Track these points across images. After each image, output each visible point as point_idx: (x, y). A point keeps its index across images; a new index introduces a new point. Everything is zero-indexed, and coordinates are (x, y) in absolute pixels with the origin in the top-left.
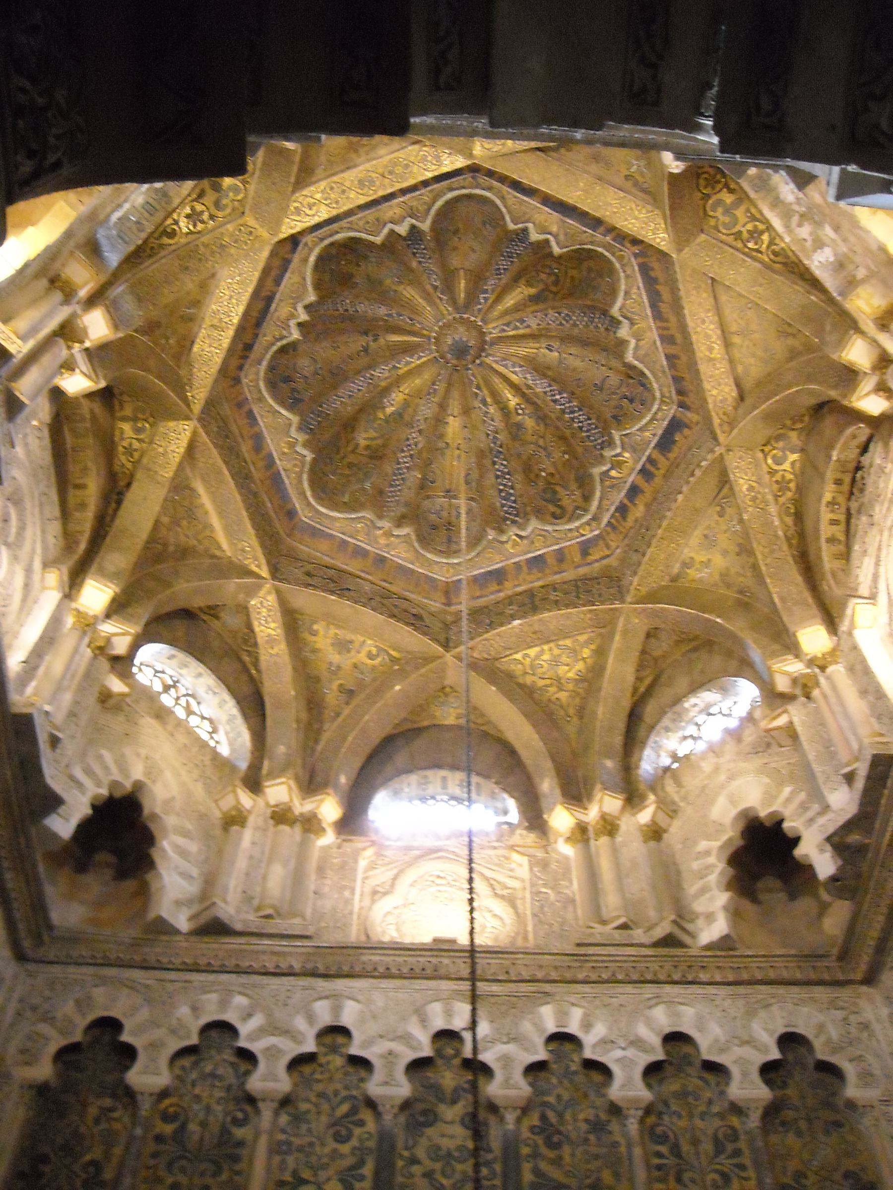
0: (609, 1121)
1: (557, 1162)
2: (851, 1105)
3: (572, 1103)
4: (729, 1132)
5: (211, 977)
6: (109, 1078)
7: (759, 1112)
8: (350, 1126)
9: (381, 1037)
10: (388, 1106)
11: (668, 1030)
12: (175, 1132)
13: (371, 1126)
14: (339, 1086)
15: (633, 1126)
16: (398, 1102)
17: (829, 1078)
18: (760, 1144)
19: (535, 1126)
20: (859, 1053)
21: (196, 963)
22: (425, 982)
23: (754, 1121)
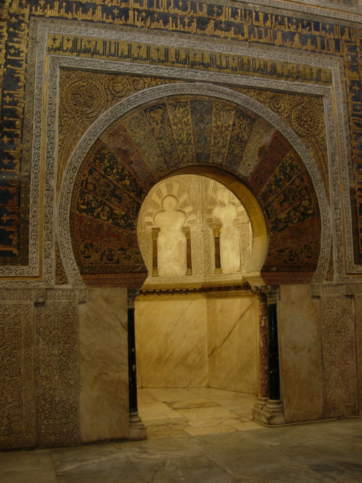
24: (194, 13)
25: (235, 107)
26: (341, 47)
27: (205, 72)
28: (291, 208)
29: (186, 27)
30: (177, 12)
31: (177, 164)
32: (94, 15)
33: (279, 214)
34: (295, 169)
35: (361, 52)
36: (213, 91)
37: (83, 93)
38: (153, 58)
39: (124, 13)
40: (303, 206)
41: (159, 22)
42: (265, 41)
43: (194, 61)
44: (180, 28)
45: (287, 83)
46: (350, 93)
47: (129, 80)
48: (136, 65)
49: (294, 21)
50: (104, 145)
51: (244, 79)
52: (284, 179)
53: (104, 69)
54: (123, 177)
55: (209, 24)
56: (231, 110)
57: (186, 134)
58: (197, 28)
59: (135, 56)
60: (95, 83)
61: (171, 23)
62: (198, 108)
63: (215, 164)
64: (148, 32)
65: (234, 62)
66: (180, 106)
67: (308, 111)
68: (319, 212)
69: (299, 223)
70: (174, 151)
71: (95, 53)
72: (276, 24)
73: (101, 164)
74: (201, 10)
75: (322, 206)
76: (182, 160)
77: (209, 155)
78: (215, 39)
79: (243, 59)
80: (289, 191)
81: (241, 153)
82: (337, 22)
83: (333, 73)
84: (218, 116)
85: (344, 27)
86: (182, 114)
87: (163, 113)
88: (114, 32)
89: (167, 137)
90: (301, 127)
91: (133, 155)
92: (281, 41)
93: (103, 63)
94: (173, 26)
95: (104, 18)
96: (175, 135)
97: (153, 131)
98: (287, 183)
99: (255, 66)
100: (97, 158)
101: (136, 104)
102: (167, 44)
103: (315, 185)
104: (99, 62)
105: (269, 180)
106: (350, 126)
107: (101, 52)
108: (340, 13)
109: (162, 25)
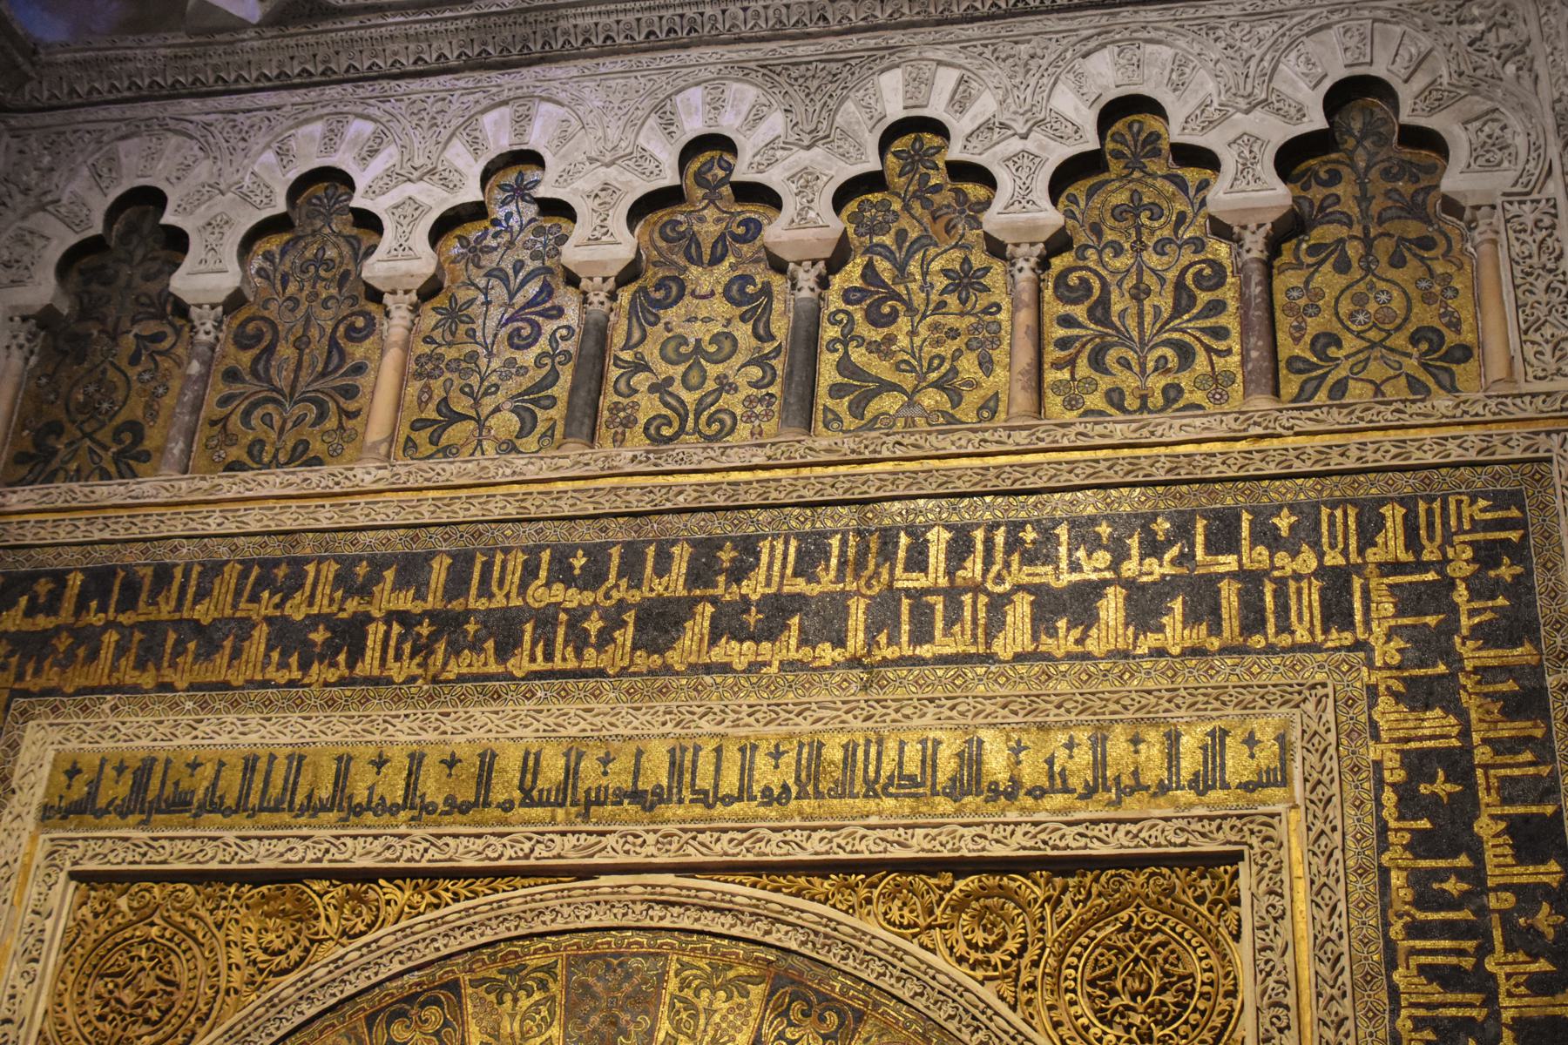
0: (987, 270)
1: (882, 349)
2: (1452, 206)
3: (924, 242)
4: (1207, 271)
5: (313, 94)
6: (153, 287)
7: (1262, 232)
8: (540, 320)
9: (592, 160)
10: (598, 280)
11: (1114, 94)
12: (256, 360)
13: (572, 316)
14: (525, 255)
15: (1025, 277)
16: (614, 270)
17: (1425, 155)
18: (1256, 290)
19: (855, 289)
20: (1489, 105)
21: (282, 74)
22: (676, 53)
23: (1255, 245)
24: (629, 587)
25: (770, 962)
26: (1357, 605)
27: (639, 829)
29: (590, 652)
30: (559, 599)
32: (235, 663)
35: (1475, 605)
36: (673, 904)
37: (143, 969)
38: (428, 800)
39: (350, 636)
41: (482, 650)
42: (947, 651)
43: (599, 789)
44: (564, 659)
45: (1035, 824)
46: (1401, 818)
47: (326, 898)
48: (355, 837)
49: (1104, 530)
51: (816, 836)
53: (234, 866)
55: (689, 624)
56: (749, 979)
58: (635, 648)
59: (361, 796)
60: (192, 925)
61: (527, 644)
62: (599, 987)
64: (430, 698)
65: (776, 767)
66: (520, 988)
67: (1159, 937)
71: (213, 804)
72: (1007, 565)
74: (662, 569)
78: (708, 679)
79: (821, 745)
82: (1334, 488)
83: (1295, 735)
84: (684, 1015)
85: (1382, 501)
86: (522, 1021)
87: (446, 1024)
88: (295, 717)
90: (1110, 1024)
92: (1028, 637)
93: (231, 841)
94: (533, 659)
95: (272, 668)
99: (878, 772)
101: (334, 995)
102: (492, 735)
104: (215, 839)
106: (1394, 992)
107: (230, 801)
108: (1356, 438)
109: (492, 660)
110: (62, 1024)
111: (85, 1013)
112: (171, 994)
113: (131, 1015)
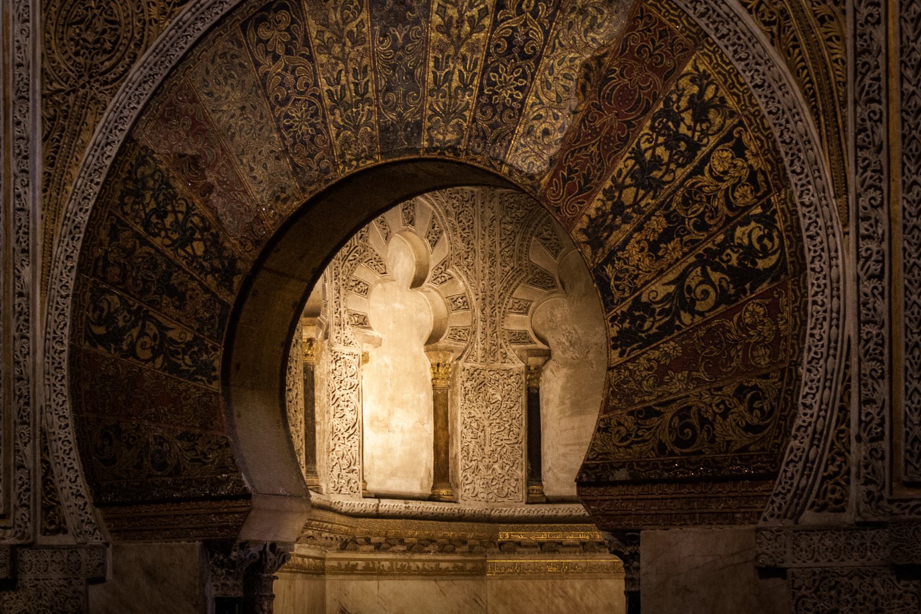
28: (692, 259)
31: (326, 171)
33: (647, 282)
34: (711, 116)
37: (94, 16)
40: (740, 246)
50: (143, 153)
52: (671, 156)
54: (188, 233)
57: (354, 69)
63: (437, 148)
68: (804, 258)
69: (722, 308)
70: (319, 132)
73: (137, 207)
75: (811, 237)
76: (342, 156)
77: (418, 125)
80: (685, 202)
81: (521, 97)
86: (342, 12)
87: (293, 21)
89: (302, 93)
91: (214, 166)
96: (322, 81)
97: (264, 84)
98: (679, 171)
100: (129, 192)
101: (217, 13)
103: (787, 161)
105: (615, 173)
110: (54, 62)
111: (66, 52)
112: (116, 30)
113: (94, 49)
